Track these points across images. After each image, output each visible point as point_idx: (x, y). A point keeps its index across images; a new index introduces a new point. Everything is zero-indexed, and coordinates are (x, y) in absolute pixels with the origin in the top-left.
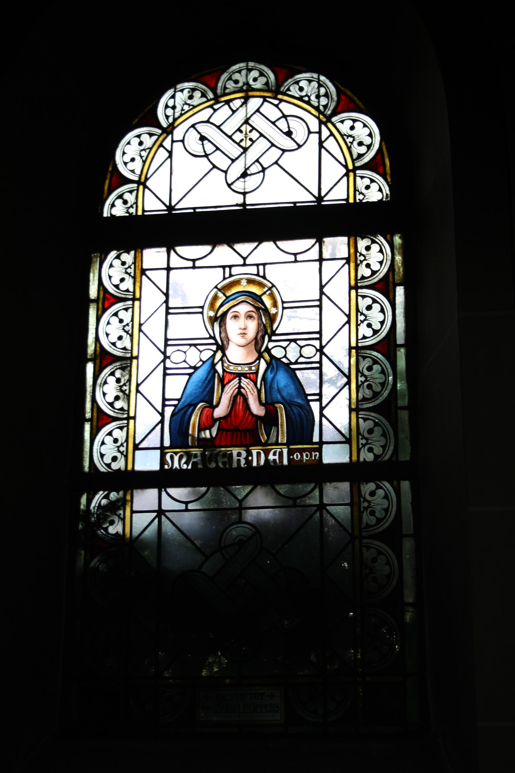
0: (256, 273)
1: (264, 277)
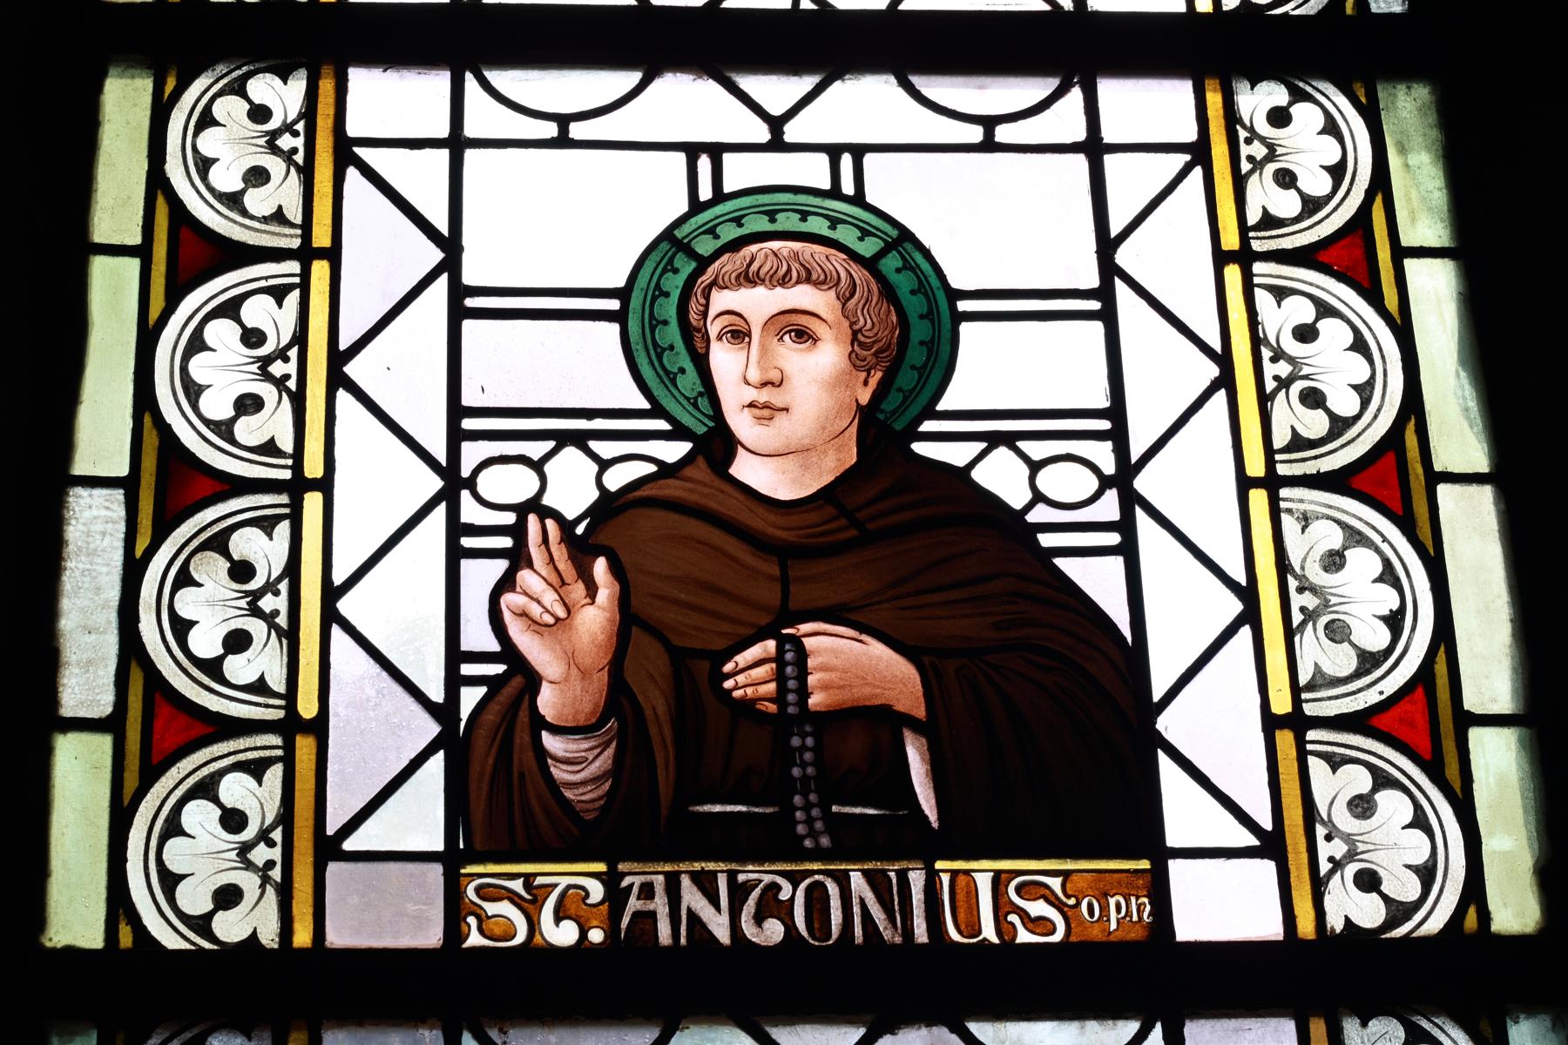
0: (826, 185)
1: (859, 199)
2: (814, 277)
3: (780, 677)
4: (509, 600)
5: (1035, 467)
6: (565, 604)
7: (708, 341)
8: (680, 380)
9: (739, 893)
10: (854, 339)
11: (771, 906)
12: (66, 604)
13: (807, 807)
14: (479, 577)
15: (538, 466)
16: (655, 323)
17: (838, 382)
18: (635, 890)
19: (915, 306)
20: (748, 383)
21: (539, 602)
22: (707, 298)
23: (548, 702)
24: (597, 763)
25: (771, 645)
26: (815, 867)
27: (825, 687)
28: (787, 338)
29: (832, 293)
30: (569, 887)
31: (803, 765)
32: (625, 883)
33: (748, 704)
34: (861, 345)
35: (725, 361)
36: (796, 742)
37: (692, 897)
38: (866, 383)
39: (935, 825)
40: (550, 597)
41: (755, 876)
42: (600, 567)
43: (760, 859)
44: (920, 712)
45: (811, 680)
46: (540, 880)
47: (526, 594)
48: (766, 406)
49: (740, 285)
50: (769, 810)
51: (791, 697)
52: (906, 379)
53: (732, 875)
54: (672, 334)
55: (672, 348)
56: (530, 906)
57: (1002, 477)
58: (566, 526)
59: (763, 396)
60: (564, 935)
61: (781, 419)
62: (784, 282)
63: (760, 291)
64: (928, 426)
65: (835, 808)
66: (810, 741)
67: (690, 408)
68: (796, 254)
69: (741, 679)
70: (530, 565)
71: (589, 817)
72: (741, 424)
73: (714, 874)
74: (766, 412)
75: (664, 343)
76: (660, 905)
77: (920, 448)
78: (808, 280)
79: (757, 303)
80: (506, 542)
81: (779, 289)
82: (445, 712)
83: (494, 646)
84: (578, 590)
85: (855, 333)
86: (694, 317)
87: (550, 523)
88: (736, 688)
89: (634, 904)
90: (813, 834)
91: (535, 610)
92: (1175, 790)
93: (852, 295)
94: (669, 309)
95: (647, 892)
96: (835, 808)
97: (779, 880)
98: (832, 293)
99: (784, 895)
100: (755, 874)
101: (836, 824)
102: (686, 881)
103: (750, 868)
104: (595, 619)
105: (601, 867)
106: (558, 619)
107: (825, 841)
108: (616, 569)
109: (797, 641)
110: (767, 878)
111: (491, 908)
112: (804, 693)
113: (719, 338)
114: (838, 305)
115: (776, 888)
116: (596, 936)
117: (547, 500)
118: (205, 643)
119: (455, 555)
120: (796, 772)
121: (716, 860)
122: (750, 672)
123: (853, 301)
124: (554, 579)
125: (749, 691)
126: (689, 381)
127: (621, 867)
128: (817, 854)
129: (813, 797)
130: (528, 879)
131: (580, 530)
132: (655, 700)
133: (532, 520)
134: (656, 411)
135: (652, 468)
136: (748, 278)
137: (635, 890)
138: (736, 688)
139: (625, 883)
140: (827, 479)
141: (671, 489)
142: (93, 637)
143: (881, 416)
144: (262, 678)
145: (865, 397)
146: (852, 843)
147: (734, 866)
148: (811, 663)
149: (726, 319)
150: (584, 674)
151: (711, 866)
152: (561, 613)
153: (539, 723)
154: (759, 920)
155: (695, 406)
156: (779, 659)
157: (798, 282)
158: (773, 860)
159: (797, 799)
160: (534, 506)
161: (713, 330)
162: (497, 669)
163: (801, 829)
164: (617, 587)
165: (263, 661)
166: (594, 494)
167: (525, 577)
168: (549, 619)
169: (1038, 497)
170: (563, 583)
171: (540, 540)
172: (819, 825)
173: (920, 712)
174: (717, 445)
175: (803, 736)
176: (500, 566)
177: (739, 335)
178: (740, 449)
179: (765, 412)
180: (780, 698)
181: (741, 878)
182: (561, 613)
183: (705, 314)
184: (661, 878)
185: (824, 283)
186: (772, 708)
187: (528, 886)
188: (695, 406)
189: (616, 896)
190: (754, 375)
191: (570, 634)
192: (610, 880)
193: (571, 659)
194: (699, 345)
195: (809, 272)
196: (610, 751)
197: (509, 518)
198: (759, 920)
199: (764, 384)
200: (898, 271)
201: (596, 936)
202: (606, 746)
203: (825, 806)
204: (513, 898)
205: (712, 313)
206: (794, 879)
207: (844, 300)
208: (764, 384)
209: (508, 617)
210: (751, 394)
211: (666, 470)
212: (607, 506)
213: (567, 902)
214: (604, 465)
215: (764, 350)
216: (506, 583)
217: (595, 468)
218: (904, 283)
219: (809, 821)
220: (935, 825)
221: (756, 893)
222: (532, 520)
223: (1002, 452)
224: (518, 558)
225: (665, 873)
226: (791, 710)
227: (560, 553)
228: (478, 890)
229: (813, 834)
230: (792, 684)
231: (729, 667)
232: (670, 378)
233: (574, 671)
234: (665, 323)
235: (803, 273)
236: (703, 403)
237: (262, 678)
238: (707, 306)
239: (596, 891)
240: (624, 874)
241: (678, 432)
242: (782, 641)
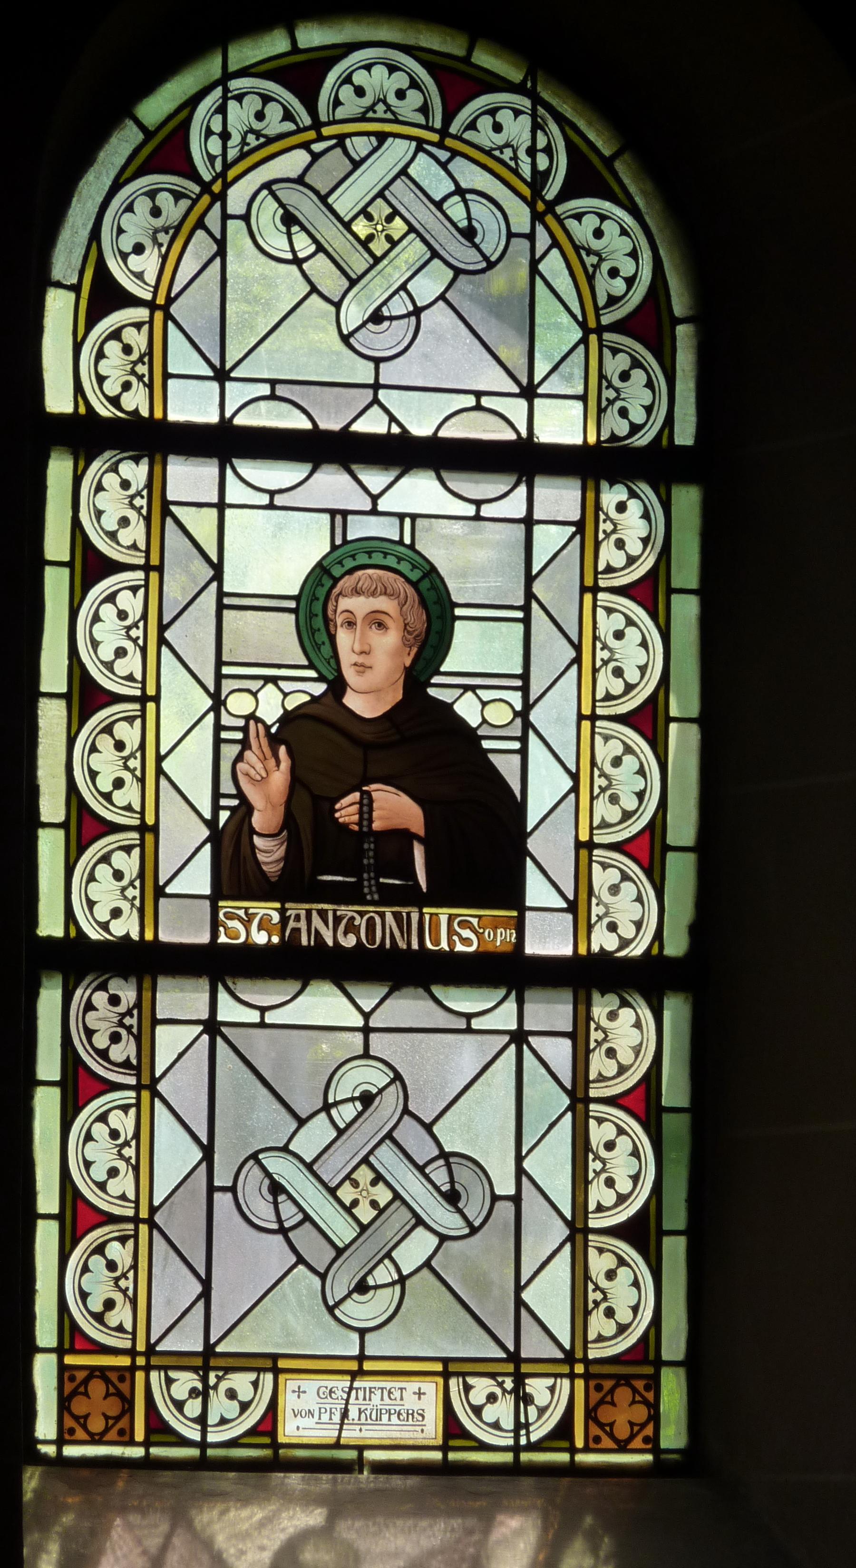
2: (388, 591)
3: (361, 813)
4: (240, 766)
5: (484, 704)
6: (266, 771)
7: (336, 627)
8: (322, 647)
9: (337, 920)
10: (405, 629)
11: (351, 928)
12: (41, 762)
13: (369, 880)
14: (229, 752)
15: (255, 694)
16: (312, 615)
17: (396, 654)
18: (293, 917)
19: (435, 610)
20: (353, 652)
21: (254, 768)
22: (337, 602)
23: (257, 820)
24: (278, 853)
25: (356, 795)
26: (371, 909)
27: (380, 818)
28: (373, 626)
29: (396, 602)
30: (264, 915)
31: (369, 858)
32: (288, 914)
33: (345, 826)
34: (409, 632)
35: (344, 638)
36: (366, 846)
37: (317, 922)
38: (409, 654)
39: (425, 890)
40: (259, 766)
41: (344, 912)
42: (282, 750)
43: (347, 903)
44: (421, 832)
45: (375, 814)
46: (251, 911)
47: (248, 763)
48: (362, 665)
49: (353, 595)
50: (352, 880)
51: (365, 823)
52: (428, 653)
53: (335, 911)
54: (319, 622)
55: (319, 630)
56: (247, 923)
57: (467, 709)
58: (267, 728)
59: (360, 659)
60: (260, 938)
61: (368, 673)
62: (373, 594)
63: (362, 599)
64: (435, 680)
65: (381, 880)
66: (372, 846)
67: (327, 665)
68: (380, 578)
69: (343, 812)
70: (250, 748)
71: (273, 880)
72: (349, 674)
73: (327, 911)
74: (361, 669)
75: (315, 627)
76: (303, 925)
77: (432, 692)
78: (385, 593)
79: (359, 605)
80: (239, 736)
81: (371, 599)
82: (211, 824)
83: (233, 791)
84: (272, 762)
85: (406, 625)
86: (330, 613)
87: (260, 725)
88: (341, 817)
89: (292, 924)
90: (371, 893)
91: (252, 772)
92: (532, 877)
93: (406, 602)
94: (318, 607)
95: (298, 918)
96: (381, 880)
97: (355, 915)
98: (396, 602)
99: (357, 923)
100: (345, 910)
101: (382, 888)
102: (314, 913)
103: (343, 908)
104: (280, 778)
105: (278, 905)
106: (262, 778)
107: (376, 897)
108: (290, 752)
109: (369, 793)
110: (350, 914)
111: (230, 924)
112: (371, 821)
113: (342, 626)
114: (399, 609)
115: (352, 919)
116: (275, 939)
117: (258, 714)
118: (105, 784)
119: (218, 742)
120: (365, 861)
121: (328, 903)
122: (347, 810)
123: (406, 606)
124: (261, 757)
125: (347, 819)
126: (326, 650)
127: (287, 905)
128: (372, 903)
129: (372, 875)
130: (247, 909)
131: (273, 730)
132: (304, 821)
133: (252, 723)
134: (311, 666)
135: (307, 698)
136: (357, 592)
137: (293, 917)
138: (341, 817)
139: (288, 914)
140: (388, 707)
141: (315, 710)
142: (56, 779)
143: (415, 673)
144: (130, 804)
145: (408, 662)
146: (389, 897)
147: (335, 907)
148: (375, 805)
149: (346, 614)
150: (274, 807)
151: (325, 906)
152: (264, 775)
153: (252, 831)
154: (345, 933)
155: (329, 663)
156: (361, 803)
157: (380, 594)
158: (353, 904)
159: (365, 876)
160: (252, 717)
161: (339, 621)
162: (235, 802)
163: (366, 890)
164: (290, 762)
165: (129, 795)
166: (281, 712)
167: (248, 754)
168: (259, 778)
169: (484, 721)
170: (265, 759)
171: (255, 735)
172: (374, 889)
173: (421, 832)
174: (337, 686)
175: (369, 843)
176: (237, 748)
177: (351, 624)
178: (349, 690)
179: (362, 668)
180: (360, 823)
181: (339, 913)
182: (264, 775)
183: (335, 611)
184: (304, 912)
185: (392, 595)
186: (356, 828)
187: (246, 913)
188: (329, 663)
189: (284, 920)
190: (357, 648)
191: (269, 785)
192: (282, 911)
193: (268, 799)
194: (332, 629)
195: (385, 588)
196: (284, 847)
197: (241, 723)
198: (345, 933)
199: (362, 653)
200: (428, 590)
201: (275, 939)
202: (282, 844)
203: (377, 879)
204: (240, 919)
205: (339, 611)
206: (361, 914)
207: (402, 606)
208: (362, 653)
209: (239, 773)
210: (355, 658)
211: (314, 699)
212: (287, 718)
213: (263, 922)
214: (286, 695)
215: (363, 634)
216: (239, 758)
217: (281, 696)
218: (431, 597)
219: (370, 886)
220: (425, 890)
221: (344, 922)
222: (252, 723)
223: (469, 694)
224: (245, 744)
225: (306, 910)
226: (365, 829)
227: (264, 741)
228: (225, 914)
229: (371, 893)
230: (366, 816)
231: (337, 806)
232: (318, 647)
233: (269, 806)
234: (316, 615)
235: (383, 590)
236: (332, 661)
237: (130, 804)
238: (336, 606)
239: (276, 917)
240: (288, 909)
241: (321, 679)
242: (363, 793)
